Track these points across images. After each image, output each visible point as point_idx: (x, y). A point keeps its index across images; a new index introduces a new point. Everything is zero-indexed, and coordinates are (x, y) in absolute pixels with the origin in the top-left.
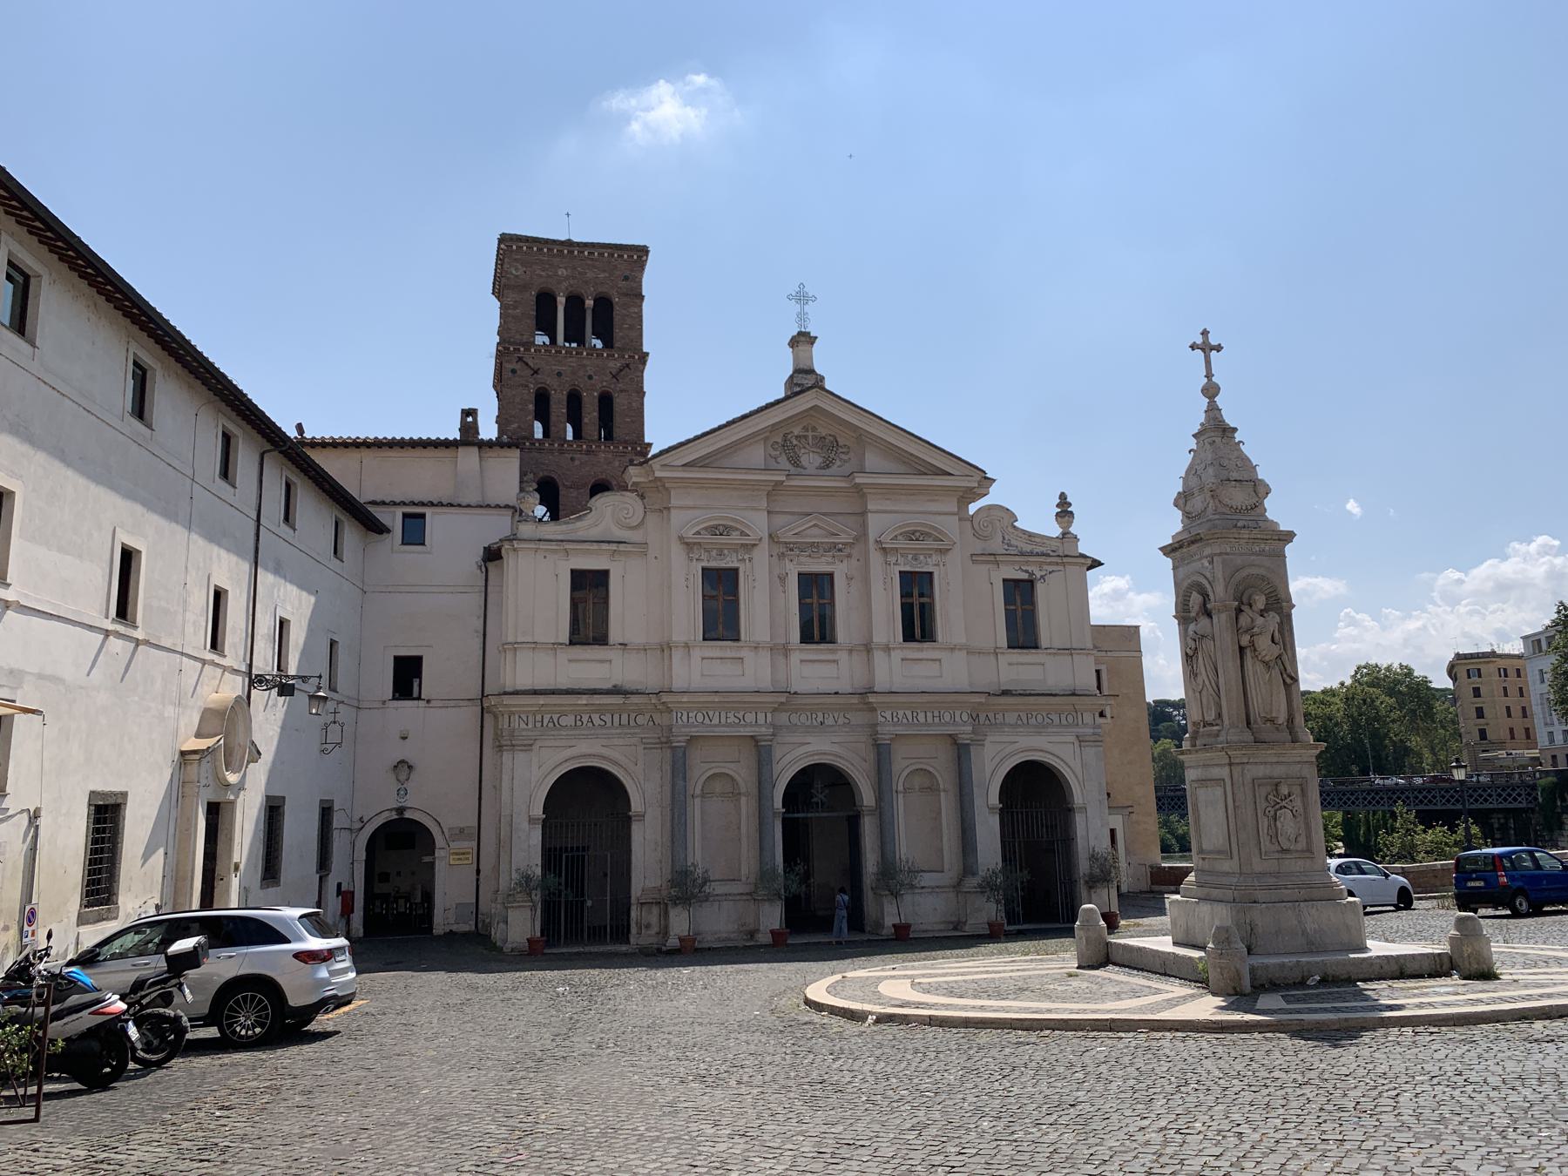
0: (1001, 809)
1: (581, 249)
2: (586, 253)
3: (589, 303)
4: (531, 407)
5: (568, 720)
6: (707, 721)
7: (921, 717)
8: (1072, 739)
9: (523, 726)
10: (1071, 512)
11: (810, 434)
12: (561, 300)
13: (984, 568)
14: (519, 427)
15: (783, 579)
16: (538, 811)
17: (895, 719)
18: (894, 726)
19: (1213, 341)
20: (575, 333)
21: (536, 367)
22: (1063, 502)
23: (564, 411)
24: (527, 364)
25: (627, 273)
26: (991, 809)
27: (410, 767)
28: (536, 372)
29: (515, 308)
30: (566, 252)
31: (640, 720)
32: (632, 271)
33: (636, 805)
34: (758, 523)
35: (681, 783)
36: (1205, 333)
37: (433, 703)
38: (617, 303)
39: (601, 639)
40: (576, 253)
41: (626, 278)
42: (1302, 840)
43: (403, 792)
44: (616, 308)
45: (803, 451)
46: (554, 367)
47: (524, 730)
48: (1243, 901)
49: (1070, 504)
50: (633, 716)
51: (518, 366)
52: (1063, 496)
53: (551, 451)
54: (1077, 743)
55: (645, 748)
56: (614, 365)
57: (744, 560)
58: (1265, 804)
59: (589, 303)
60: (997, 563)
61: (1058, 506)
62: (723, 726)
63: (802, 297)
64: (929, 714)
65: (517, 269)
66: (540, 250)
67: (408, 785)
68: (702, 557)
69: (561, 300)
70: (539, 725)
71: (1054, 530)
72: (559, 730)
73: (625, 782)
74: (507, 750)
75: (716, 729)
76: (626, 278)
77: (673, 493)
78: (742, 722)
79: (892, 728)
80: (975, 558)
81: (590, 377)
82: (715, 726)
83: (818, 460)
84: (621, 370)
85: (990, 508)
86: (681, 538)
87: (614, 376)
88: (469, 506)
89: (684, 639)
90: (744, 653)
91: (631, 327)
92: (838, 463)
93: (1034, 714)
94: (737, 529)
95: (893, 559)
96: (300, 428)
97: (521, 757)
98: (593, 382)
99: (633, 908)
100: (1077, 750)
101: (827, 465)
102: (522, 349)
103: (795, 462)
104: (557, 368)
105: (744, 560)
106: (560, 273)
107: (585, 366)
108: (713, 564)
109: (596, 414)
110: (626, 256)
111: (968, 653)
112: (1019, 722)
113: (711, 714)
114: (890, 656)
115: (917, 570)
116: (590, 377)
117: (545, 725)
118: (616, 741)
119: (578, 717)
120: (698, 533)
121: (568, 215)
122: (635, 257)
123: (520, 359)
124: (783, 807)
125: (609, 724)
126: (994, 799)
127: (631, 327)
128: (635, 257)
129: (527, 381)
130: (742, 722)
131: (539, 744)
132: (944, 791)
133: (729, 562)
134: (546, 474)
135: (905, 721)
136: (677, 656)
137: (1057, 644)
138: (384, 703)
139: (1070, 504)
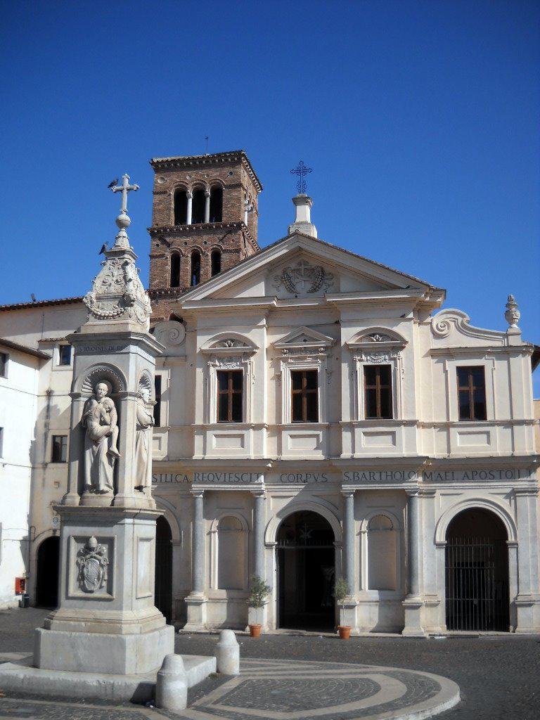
2: (204, 162)
3: (208, 192)
6: (216, 479)
7: (377, 476)
11: (302, 267)
12: (190, 193)
14: (160, 282)
15: (278, 378)
24: (165, 240)
29: (159, 204)
31: (179, 478)
34: (263, 338)
45: (297, 280)
50: (174, 477)
51: (159, 242)
55: (182, 498)
59: (208, 192)
63: (301, 171)
64: (384, 475)
66: (175, 165)
69: (190, 193)
78: (241, 481)
80: (434, 353)
83: (309, 286)
91: (233, 206)
92: (324, 287)
93: (479, 472)
96: (32, 296)
101: (314, 290)
103: (291, 288)
106: (188, 178)
108: (223, 368)
113: (219, 474)
115: (378, 364)
116: (205, 243)
118: (163, 493)
120: (214, 346)
122: (236, 159)
126: (441, 537)
128: (236, 159)
130: (241, 481)
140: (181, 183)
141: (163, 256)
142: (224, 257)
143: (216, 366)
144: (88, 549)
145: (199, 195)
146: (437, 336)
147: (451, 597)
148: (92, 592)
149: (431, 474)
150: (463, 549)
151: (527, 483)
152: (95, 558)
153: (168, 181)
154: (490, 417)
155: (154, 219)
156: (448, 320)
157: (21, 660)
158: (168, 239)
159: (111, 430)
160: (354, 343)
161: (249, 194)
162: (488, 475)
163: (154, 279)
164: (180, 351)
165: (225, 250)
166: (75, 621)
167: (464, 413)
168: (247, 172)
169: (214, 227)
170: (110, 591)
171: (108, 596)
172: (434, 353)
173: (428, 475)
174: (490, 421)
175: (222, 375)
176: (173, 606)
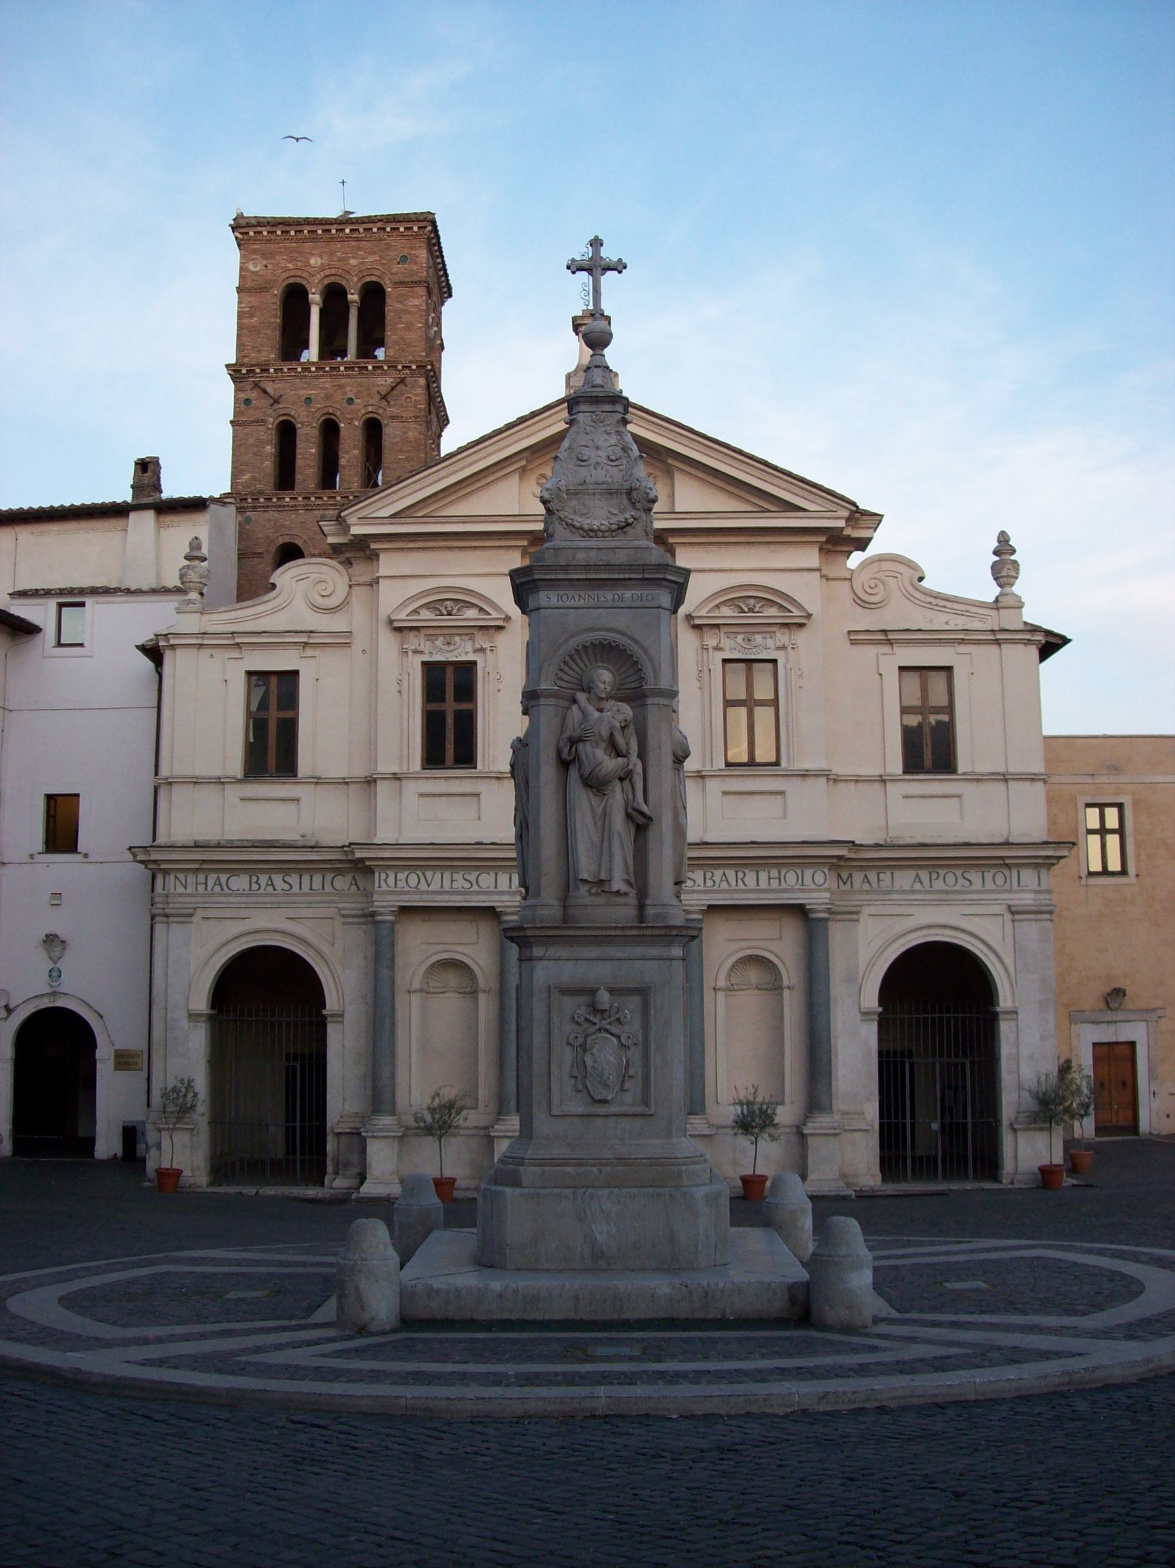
0: (880, 1014)
2: (347, 231)
3: (353, 297)
4: (270, 449)
5: (240, 882)
6: (423, 886)
8: (1001, 909)
9: (180, 889)
10: (1015, 562)
12: (315, 298)
13: (871, 651)
14: (253, 478)
16: (201, 1002)
17: (710, 883)
18: (705, 892)
19: (609, 253)
20: (332, 347)
21: (278, 394)
22: (1004, 547)
23: (313, 451)
24: (265, 392)
25: (405, 252)
26: (866, 1014)
27: (63, 942)
28: (276, 401)
29: (252, 316)
30: (320, 232)
32: (412, 249)
33: (332, 1003)
35: (385, 972)
36: (596, 243)
37: (90, 859)
39: (287, 766)
40: (334, 231)
41: (404, 259)
42: (634, 1087)
43: (55, 974)
44: (389, 301)
46: (301, 392)
47: (181, 895)
48: (1073, 1165)
49: (1013, 551)
51: (253, 395)
52: (1003, 538)
53: (294, 509)
54: (1008, 917)
55: (344, 924)
56: (384, 382)
57: (482, 650)
58: (568, 1028)
59: (353, 297)
60: (890, 642)
61: (996, 553)
62: (447, 892)
65: (256, 265)
67: (59, 965)
68: (422, 648)
69: (315, 298)
70: (201, 888)
71: (989, 591)
72: (228, 895)
73: (317, 969)
74: (161, 922)
75: (439, 898)
76: (404, 259)
77: (382, 556)
79: (703, 896)
80: (855, 638)
81: (350, 401)
82: (434, 892)
84: (393, 389)
85: (881, 559)
86: (391, 622)
87: (384, 397)
88: (139, 592)
89: (395, 769)
90: (481, 787)
91: (409, 327)
94: (474, 605)
95: (711, 640)
97: (177, 931)
98: (352, 407)
99: (329, 1138)
100: (1008, 925)
102: (258, 371)
104: (305, 393)
105: (482, 650)
106: (313, 261)
107: (341, 387)
108: (438, 658)
109: (356, 452)
110: (402, 229)
111: (828, 780)
112: (917, 886)
114: (704, 788)
116: (350, 401)
117: (209, 888)
119: (254, 879)
120: (416, 611)
121: (343, 182)
123: (256, 385)
124: (880, 1005)
125: (296, 889)
126: (871, 999)
127: (409, 327)
128: (415, 229)
129: (265, 414)
130: (475, 888)
131: (200, 913)
132: (789, 988)
133: (462, 652)
134: (287, 540)
135: (724, 885)
136: (382, 788)
137: (982, 768)
138: (32, 856)
139: (1013, 551)
140: (300, 273)
142: (391, 433)
143: (422, 652)
144: (595, 1009)
145: (334, 295)
146: (863, 604)
147: (889, 1117)
148: (604, 1102)
149: (850, 876)
150: (918, 1025)
151: (1032, 896)
152: (606, 1031)
153: (270, 266)
154: (963, 765)
155: (240, 347)
156: (881, 575)
157: (786, 1241)
159: (630, 767)
160: (703, 613)
162: (960, 880)
163: (241, 472)
164: (336, 623)
165: (393, 417)
166: (575, 1165)
167: (914, 763)
169: (370, 368)
170: (646, 1102)
171: (644, 1110)
172: (855, 638)
173: (845, 875)
174: (964, 774)
175: (433, 672)
176: (329, 1148)
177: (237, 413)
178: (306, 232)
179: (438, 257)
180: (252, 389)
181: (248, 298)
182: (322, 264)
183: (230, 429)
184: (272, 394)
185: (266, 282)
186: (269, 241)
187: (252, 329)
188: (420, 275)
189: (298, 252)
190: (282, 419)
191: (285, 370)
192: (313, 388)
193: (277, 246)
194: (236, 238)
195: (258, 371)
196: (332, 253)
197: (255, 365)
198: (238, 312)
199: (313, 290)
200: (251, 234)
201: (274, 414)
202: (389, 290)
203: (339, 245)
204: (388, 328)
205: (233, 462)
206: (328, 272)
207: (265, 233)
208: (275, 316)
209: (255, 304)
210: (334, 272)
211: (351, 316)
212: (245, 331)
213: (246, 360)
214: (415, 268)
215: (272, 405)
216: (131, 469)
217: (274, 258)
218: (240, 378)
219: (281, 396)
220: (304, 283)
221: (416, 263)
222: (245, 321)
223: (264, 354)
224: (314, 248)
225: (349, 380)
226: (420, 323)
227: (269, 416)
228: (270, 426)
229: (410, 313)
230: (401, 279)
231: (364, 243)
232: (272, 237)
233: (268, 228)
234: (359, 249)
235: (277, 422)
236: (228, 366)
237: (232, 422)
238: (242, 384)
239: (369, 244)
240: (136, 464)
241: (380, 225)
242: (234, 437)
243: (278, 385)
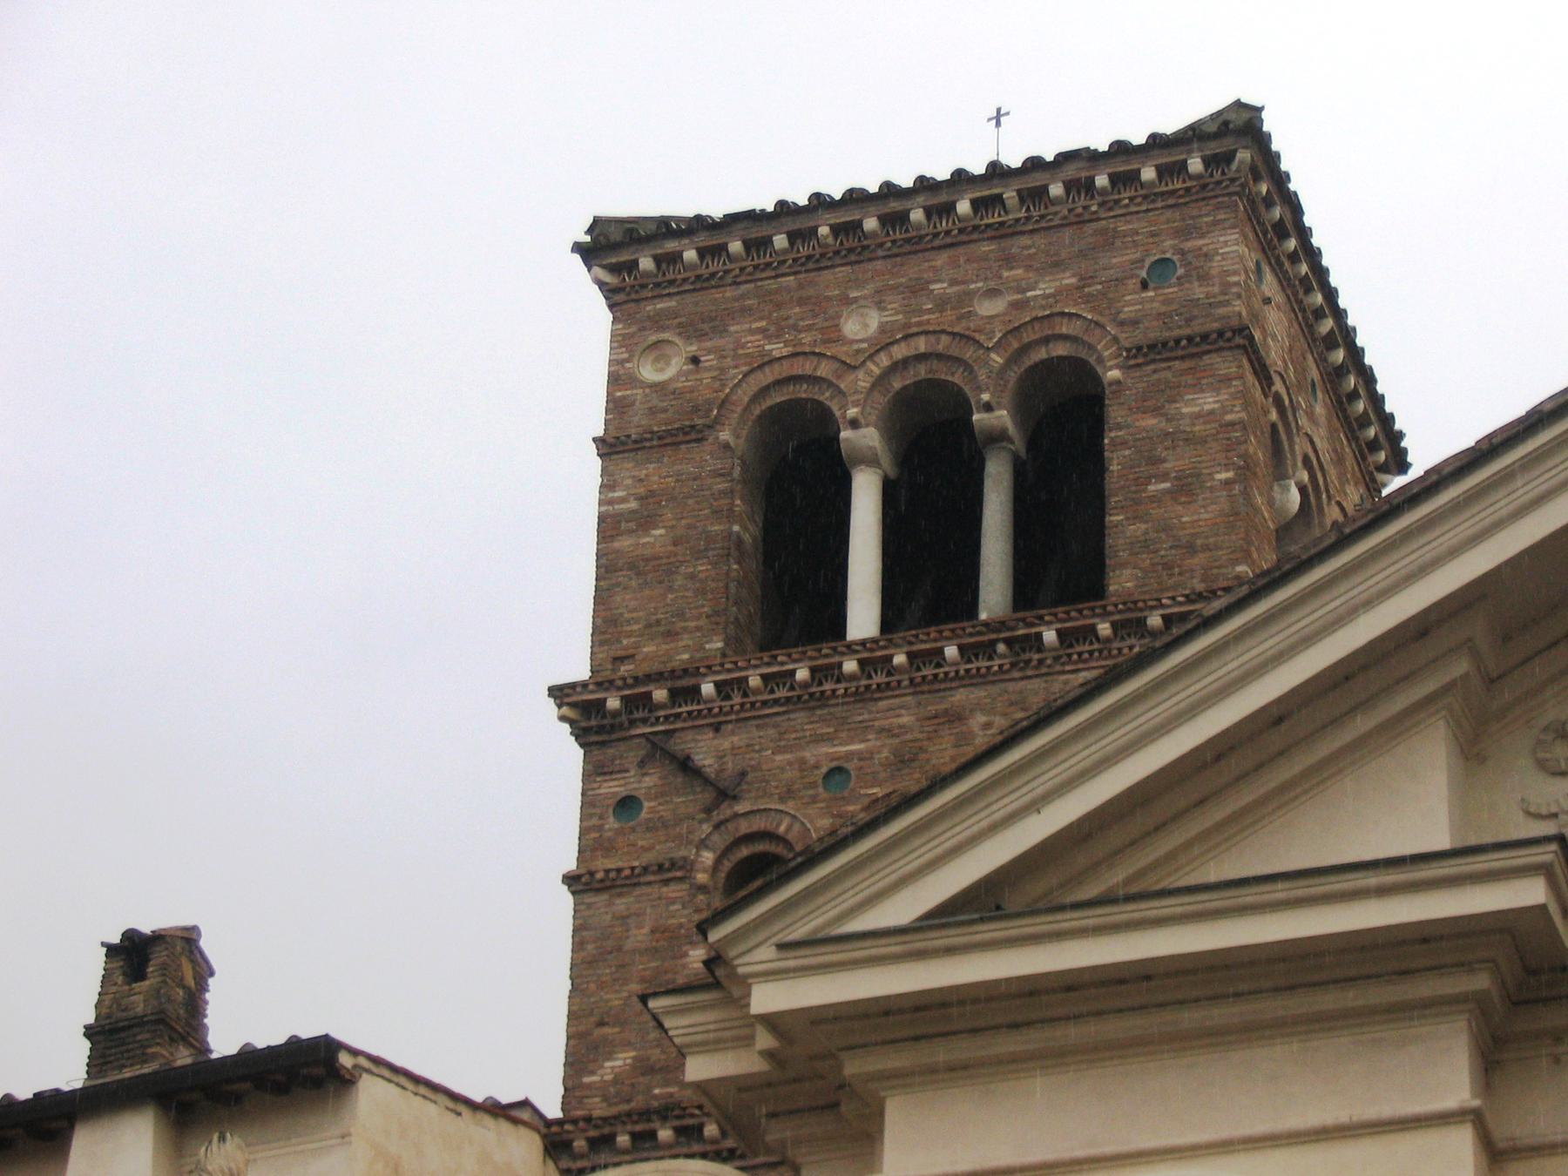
1: (943, 198)
2: (963, 207)
21: (731, 765)
24: (686, 766)
28: (725, 795)
29: (645, 521)
32: (1184, 233)
38: (1118, 382)
44: (1115, 413)
46: (809, 754)
51: (644, 783)
91: (1186, 487)
102: (660, 695)
104: (822, 754)
107: (955, 717)
122: (1195, 165)
123: (660, 752)
140: (804, 367)
141: (670, 870)
153: (708, 360)
155: (606, 626)
158: (706, 751)
161: (1301, 446)
163: (604, 1049)
168: (1278, 268)
169: (1050, 636)
177: (592, 839)
178: (824, 230)
179: (1294, 258)
180: (642, 764)
181: (628, 469)
182: (883, 329)
183: (565, 900)
184: (710, 772)
185: (696, 409)
186: (702, 283)
187: (639, 566)
188: (1222, 311)
189: (801, 302)
190: (744, 852)
191: (754, 681)
192: (860, 732)
193: (730, 293)
194: (601, 285)
195: (660, 695)
196: (917, 288)
197: (649, 678)
198: (602, 519)
199: (852, 412)
200: (646, 263)
201: (720, 840)
202: (1114, 374)
203: (941, 259)
204: (1113, 501)
205: (572, 1016)
206: (899, 352)
207: (690, 255)
208: (730, 515)
209: (655, 483)
210: (921, 345)
211: (989, 485)
212: (621, 577)
213: (625, 669)
214: (1198, 291)
215: (708, 811)
216: (94, 965)
217: (722, 331)
218: (601, 730)
219: (743, 774)
220: (825, 397)
221: (1204, 278)
222: (624, 543)
223: (686, 640)
224: (859, 284)
225: (979, 693)
226: (1227, 467)
227: (703, 844)
228: (702, 877)
229: (1190, 440)
230: (1154, 335)
231: (1025, 240)
232: (716, 266)
233: (703, 239)
234: (1008, 261)
235: (727, 865)
236: (559, 693)
237: (570, 880)
238: (611, 751)
239: (1040, 241)
240: (111, 951)
241: (1071, 171)
242: (576, 931)
243: (731, 740)
